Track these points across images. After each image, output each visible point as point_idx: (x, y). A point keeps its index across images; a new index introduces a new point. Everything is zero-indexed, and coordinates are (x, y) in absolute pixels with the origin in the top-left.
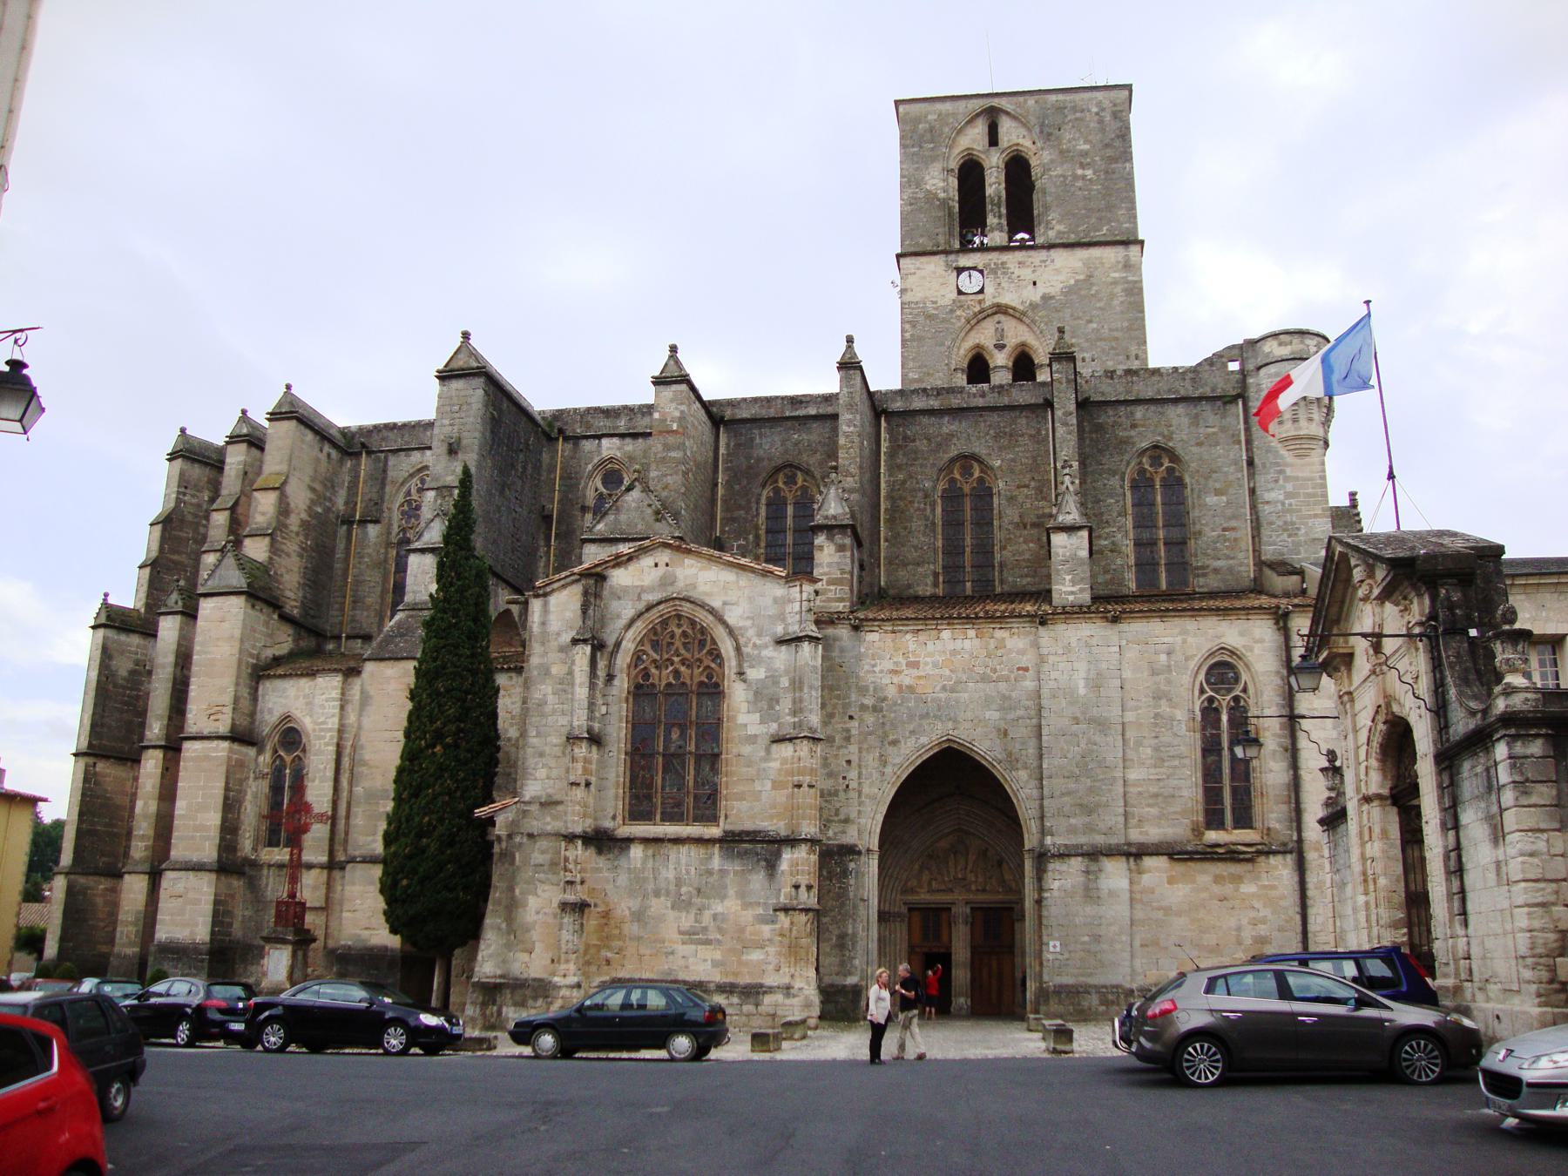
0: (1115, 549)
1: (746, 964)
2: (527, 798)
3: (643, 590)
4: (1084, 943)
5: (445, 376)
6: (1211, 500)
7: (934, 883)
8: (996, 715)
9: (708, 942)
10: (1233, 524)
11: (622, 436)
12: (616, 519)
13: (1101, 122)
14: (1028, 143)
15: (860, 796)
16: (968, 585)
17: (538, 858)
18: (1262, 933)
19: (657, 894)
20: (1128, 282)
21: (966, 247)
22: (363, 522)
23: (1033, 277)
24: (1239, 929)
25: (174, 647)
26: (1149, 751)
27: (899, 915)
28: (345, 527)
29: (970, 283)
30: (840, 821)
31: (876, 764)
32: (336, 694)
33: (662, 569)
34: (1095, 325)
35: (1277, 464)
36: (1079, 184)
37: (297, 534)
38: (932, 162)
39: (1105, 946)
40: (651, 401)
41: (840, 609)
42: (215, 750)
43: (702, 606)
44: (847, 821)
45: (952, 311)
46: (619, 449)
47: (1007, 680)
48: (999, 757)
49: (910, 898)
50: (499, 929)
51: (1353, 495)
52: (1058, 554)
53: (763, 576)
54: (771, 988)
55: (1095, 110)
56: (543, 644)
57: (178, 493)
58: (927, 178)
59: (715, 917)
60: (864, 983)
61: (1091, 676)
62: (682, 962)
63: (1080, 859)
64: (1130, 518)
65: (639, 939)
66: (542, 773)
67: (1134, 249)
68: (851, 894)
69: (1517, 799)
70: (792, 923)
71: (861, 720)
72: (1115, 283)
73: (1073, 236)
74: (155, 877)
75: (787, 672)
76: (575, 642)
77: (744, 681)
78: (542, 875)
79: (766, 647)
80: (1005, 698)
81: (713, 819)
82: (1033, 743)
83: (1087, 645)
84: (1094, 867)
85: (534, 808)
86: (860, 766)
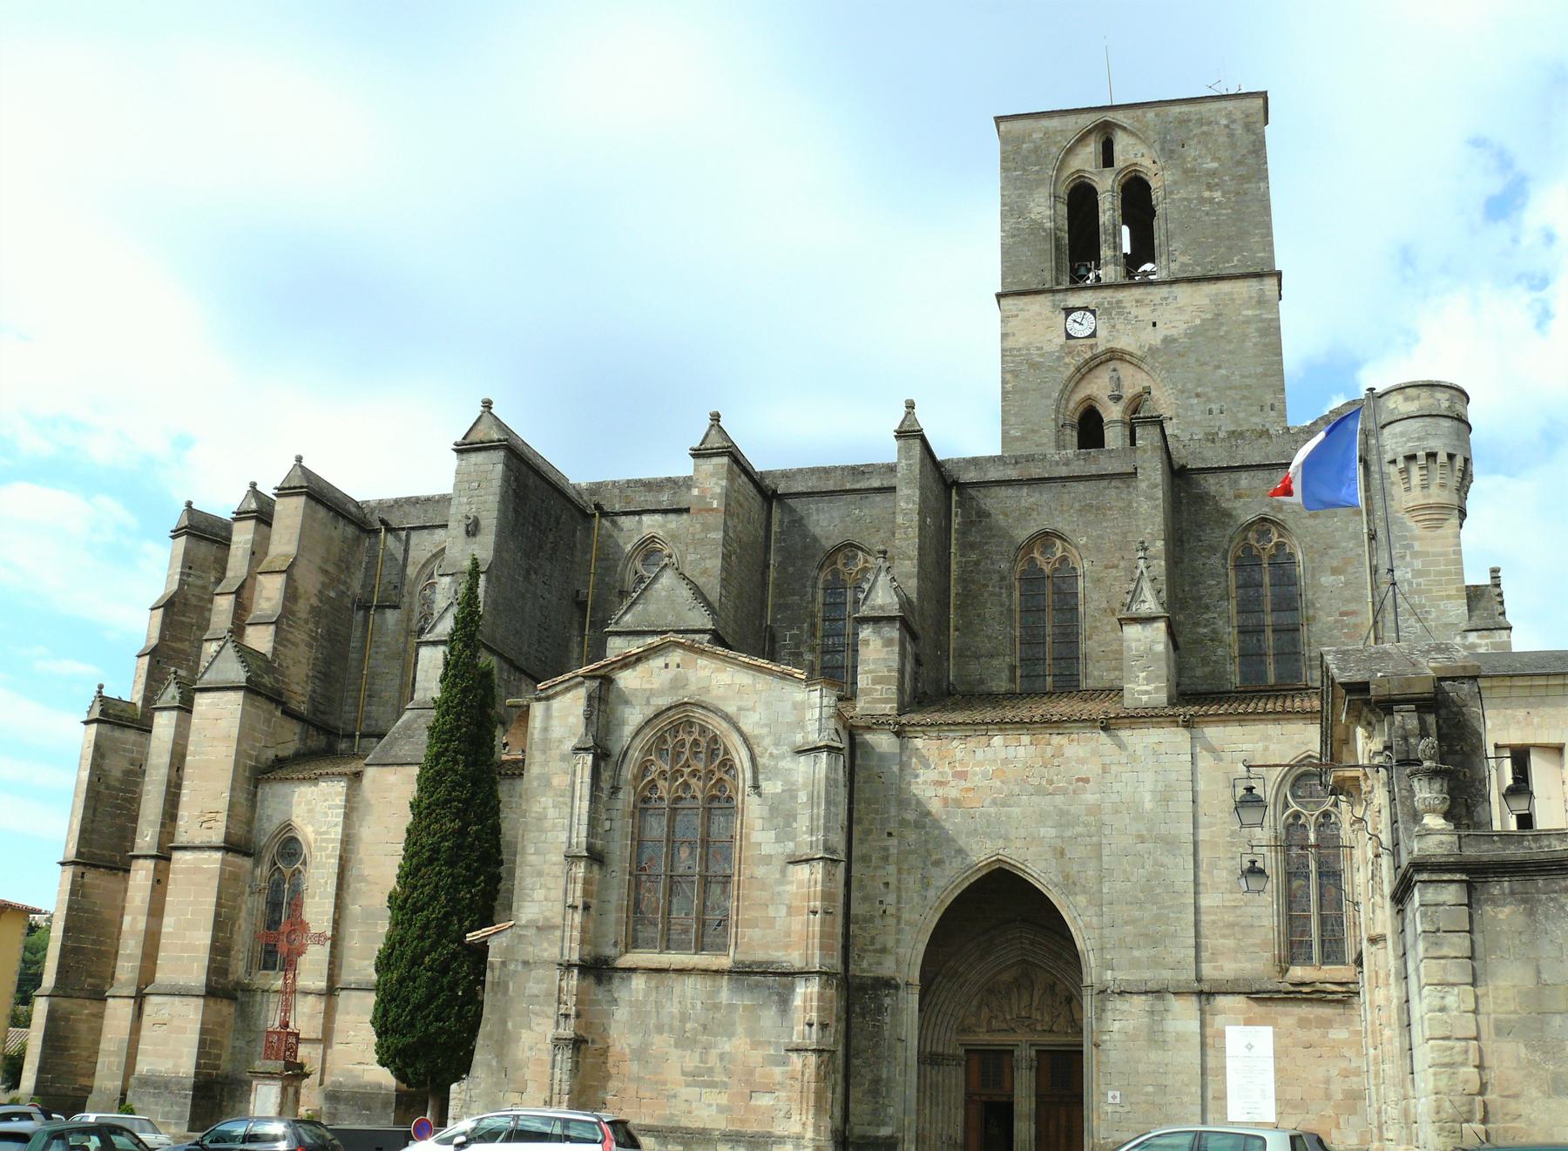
0: (1215, 638)
1: (755, 1110)
2: (523, 922)
3: (653, 693)
4: (1147, 1094)
5: (463, 449)
6: (1327, 580)
7: (994, 1021)
8: (1052, 832)
9: (711, 1085)
10: (1353, 607)
11: (665, 512)
12: (645, 609)
13: (1231, 135)
14: (1147, 162)
15: (899, 922)
16: (1049, 679)
17: (533, 988)
18: (1355, 1087)
19: (660, 1029)
20: (1263, 321)
21: (1077, 280)
22: (381, 607)
23: (1153, 318)
24: (1328, 1081)
25: (169, 746)
26: (1224, 874)
27: (954, 1057)
28: (361, 613)
29: (1082, 326)
30: (876, 951)
31: (918, 886)
32: (340, 800)
33: (672, 671)
34: (1223, 372)
35: (1404, 538)
36: (1207, 208)
37: (307, 622)
38: (1037, 187)
39: (1172, 1099)
40: (690, 472)
41: (887, 711)
43: (716, 711)
44: (883, 950)
45: (1059, 358)
46: (661, 526)
47: (1064, 792)
48: (1055, 880)
49: (970, 1038)
50: (489, 1066)
51: (1495, 572)
52: (1130, 648)
53: (781, 678)
54: (780, 1137)
55: (1224, 122)
56: (544, 752)
57: (182, 574)
58: (1032, 205)
59: (722, 1057)
60: (900, 1135)
61: (1159, 788)
62: (684, 1107)
63: (1143, 997)
64: (1234, 602)
65: (639, 1079)
66: (539, 894)
67: (1270, 283)
68: (887, 1034)
69: (1426, 950)
70: (804, 1065)
71: (901, 837)
72: (1248, 321)
73: (1199, 269)
74: (140, 998)
75: (805, 785)
76: (577, 750)
77: (760, 795)
78: (537, 1007)
79: (783, 757)
80: (1062, 813)
81: (722, 948)
82: (1092, 865)
83: (1155, 752)
84: (1159, 1006)
85: (531, 932)
86: (899, 889)
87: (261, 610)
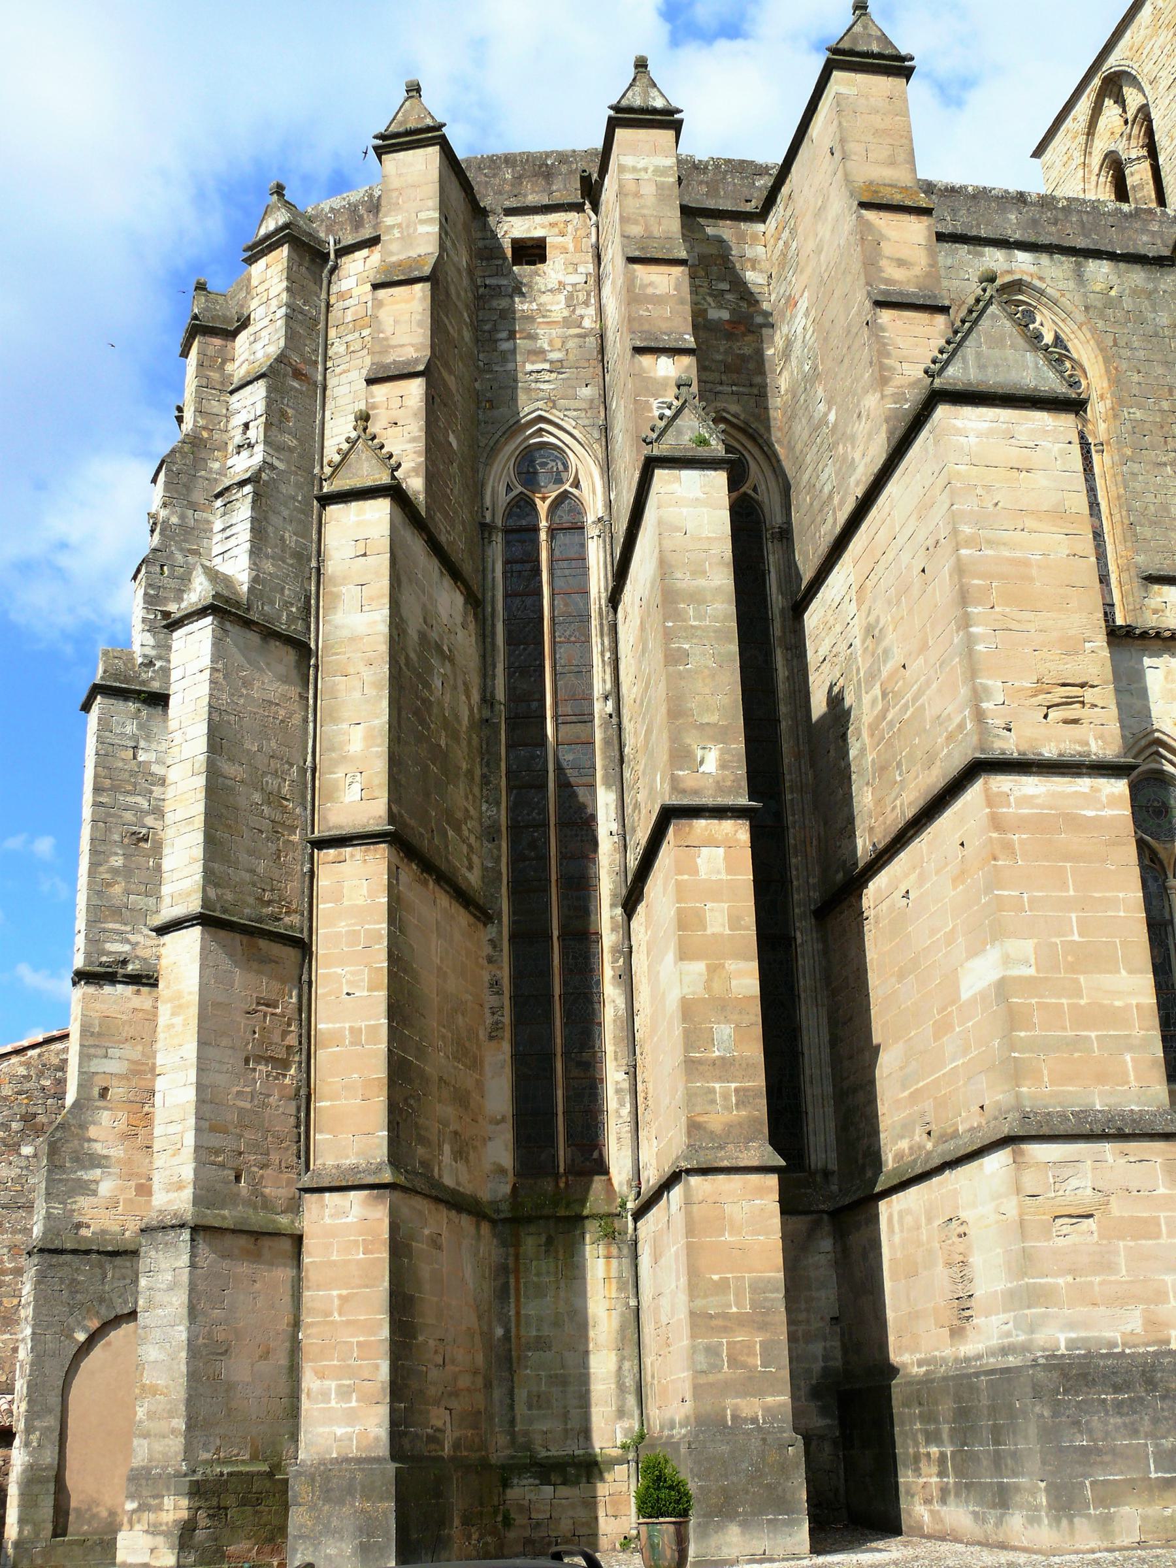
42: (1090, 799)
87: (887, 281)
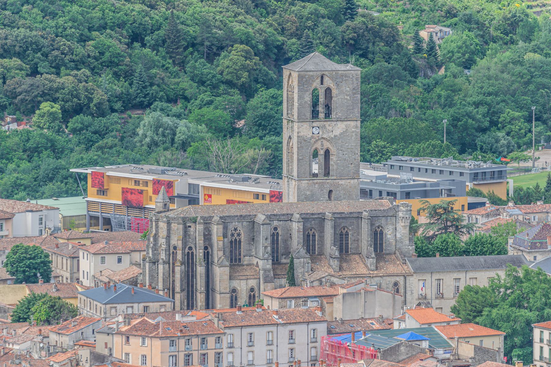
14: (332, 85)
72: (353, 132)
